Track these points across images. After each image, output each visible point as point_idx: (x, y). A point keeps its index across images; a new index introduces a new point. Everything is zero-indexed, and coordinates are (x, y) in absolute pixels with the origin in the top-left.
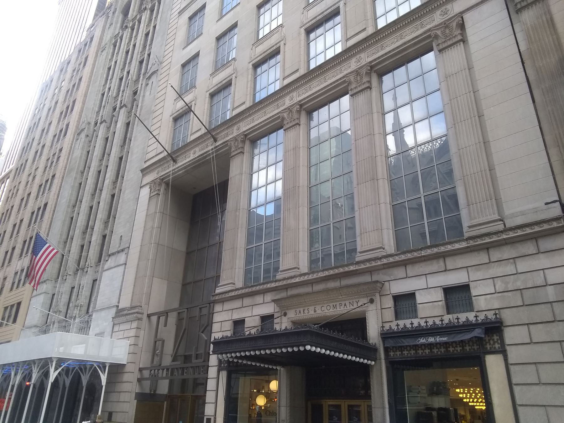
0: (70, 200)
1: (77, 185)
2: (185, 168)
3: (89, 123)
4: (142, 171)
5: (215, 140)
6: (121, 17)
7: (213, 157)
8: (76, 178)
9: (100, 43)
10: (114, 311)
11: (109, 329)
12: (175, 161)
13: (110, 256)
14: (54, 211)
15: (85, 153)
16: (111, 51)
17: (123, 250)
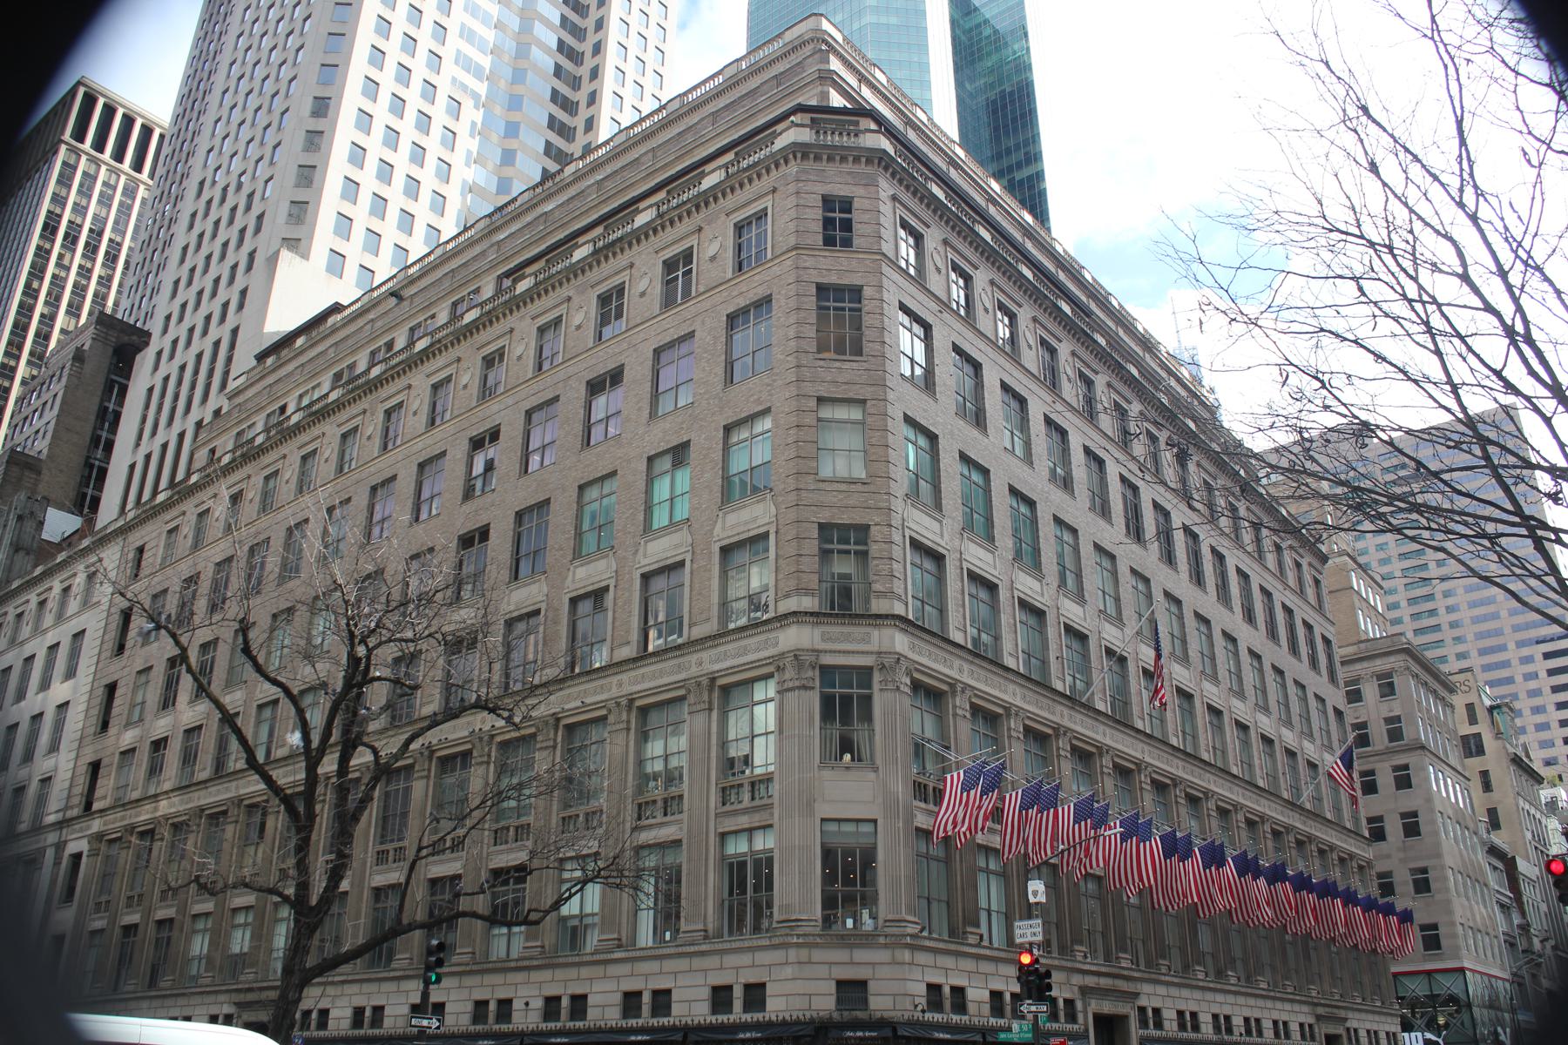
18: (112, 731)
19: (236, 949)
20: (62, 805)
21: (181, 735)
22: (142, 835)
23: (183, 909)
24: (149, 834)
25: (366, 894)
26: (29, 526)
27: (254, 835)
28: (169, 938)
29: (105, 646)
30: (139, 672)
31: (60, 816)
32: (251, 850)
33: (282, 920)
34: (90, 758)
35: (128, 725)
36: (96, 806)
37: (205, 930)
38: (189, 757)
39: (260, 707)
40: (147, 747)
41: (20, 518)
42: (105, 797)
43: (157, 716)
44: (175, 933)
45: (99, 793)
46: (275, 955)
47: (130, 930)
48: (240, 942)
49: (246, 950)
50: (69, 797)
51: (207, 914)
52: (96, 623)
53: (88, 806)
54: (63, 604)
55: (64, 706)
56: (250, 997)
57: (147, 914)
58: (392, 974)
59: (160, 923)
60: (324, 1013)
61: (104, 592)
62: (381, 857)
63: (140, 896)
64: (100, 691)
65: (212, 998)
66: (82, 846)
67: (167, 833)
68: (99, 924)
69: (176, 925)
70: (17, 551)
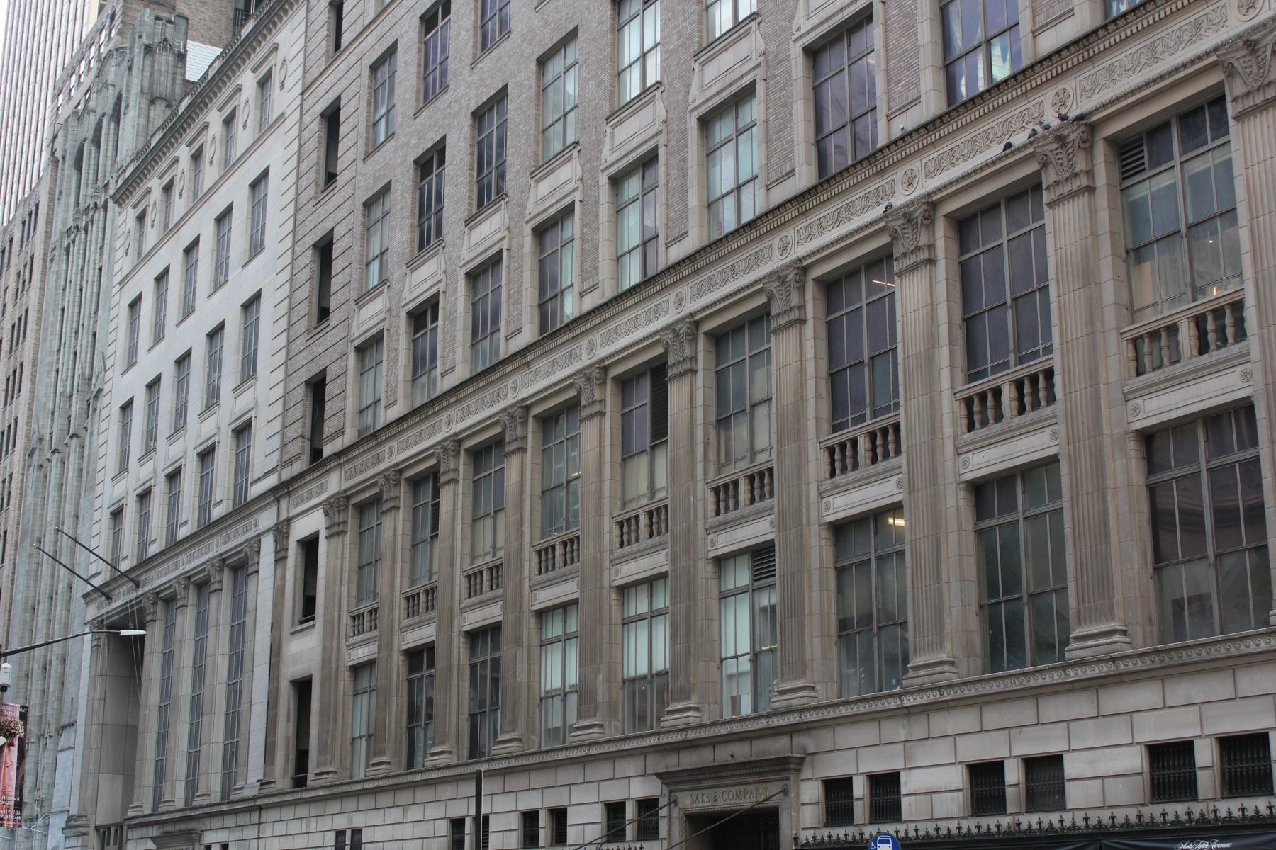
0: (27, 598)
1: (34, 567)
2: (119, 613)
3: (41, 440)
4: (85, 596)
5: (137, 585)
6: (75, 173)
7: (133, 613)
8: (31, 555)
9: (48, 235)
10: (65, 817)
11: (62, 844)
12: (109, 598)
13: (63, 728)
14: (10, 611)
15: (39, 501)
16: (64, 266)
17: (72, 724)
18: (334, 318)
19: (637, 665)
20: (273, 461)
21: (462, 285)
22: (416, 483)
23: (514, 604)
24: (426, 481)
25: (956, 504)
26: (164, 60)
27: (642, 434)
28: (496, 662)
29: (303, 183)
30: (368, 205)
31: (272, 481)
32: (644, 461)
33: (737, 592)
34: (304, 375)
35: (364, 298)
36: (328, 450)
37: (567, 638)
38: (483, 324)
39: (616, 181)
40: (403, 324)
41: (148, 49)
42: (341, 432)
43: (412, 265)
44: (507, 650)
45: (329, 427)
46: (730, 667)
47: (419, 657)
48: (646, 651)
49: (661, 663)
50: (284, 445)
51: (565, 607)
52: (283, 154)
53: (316, 454)
54: (228, 141)
55: (251, 305)
56: (690, 760)
57: (446, 626)
58: (1073, 674)
59: (475, 636)
60: (886, 787)
61: (284, 99)
62: (979, 410)
63: (431, 591)
64: (308, 258)
65: (604, 770)
66: (312, 523)
67: (463, 465)
68: (362, 654)
69: (507, 633)
70: (152, 102)
